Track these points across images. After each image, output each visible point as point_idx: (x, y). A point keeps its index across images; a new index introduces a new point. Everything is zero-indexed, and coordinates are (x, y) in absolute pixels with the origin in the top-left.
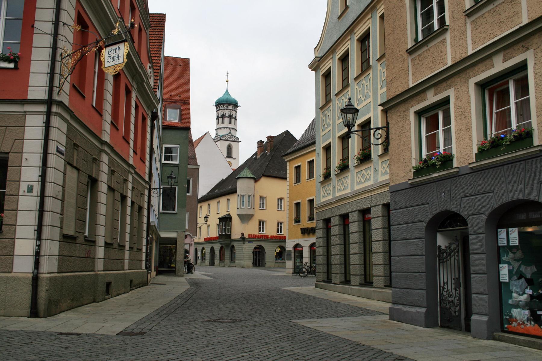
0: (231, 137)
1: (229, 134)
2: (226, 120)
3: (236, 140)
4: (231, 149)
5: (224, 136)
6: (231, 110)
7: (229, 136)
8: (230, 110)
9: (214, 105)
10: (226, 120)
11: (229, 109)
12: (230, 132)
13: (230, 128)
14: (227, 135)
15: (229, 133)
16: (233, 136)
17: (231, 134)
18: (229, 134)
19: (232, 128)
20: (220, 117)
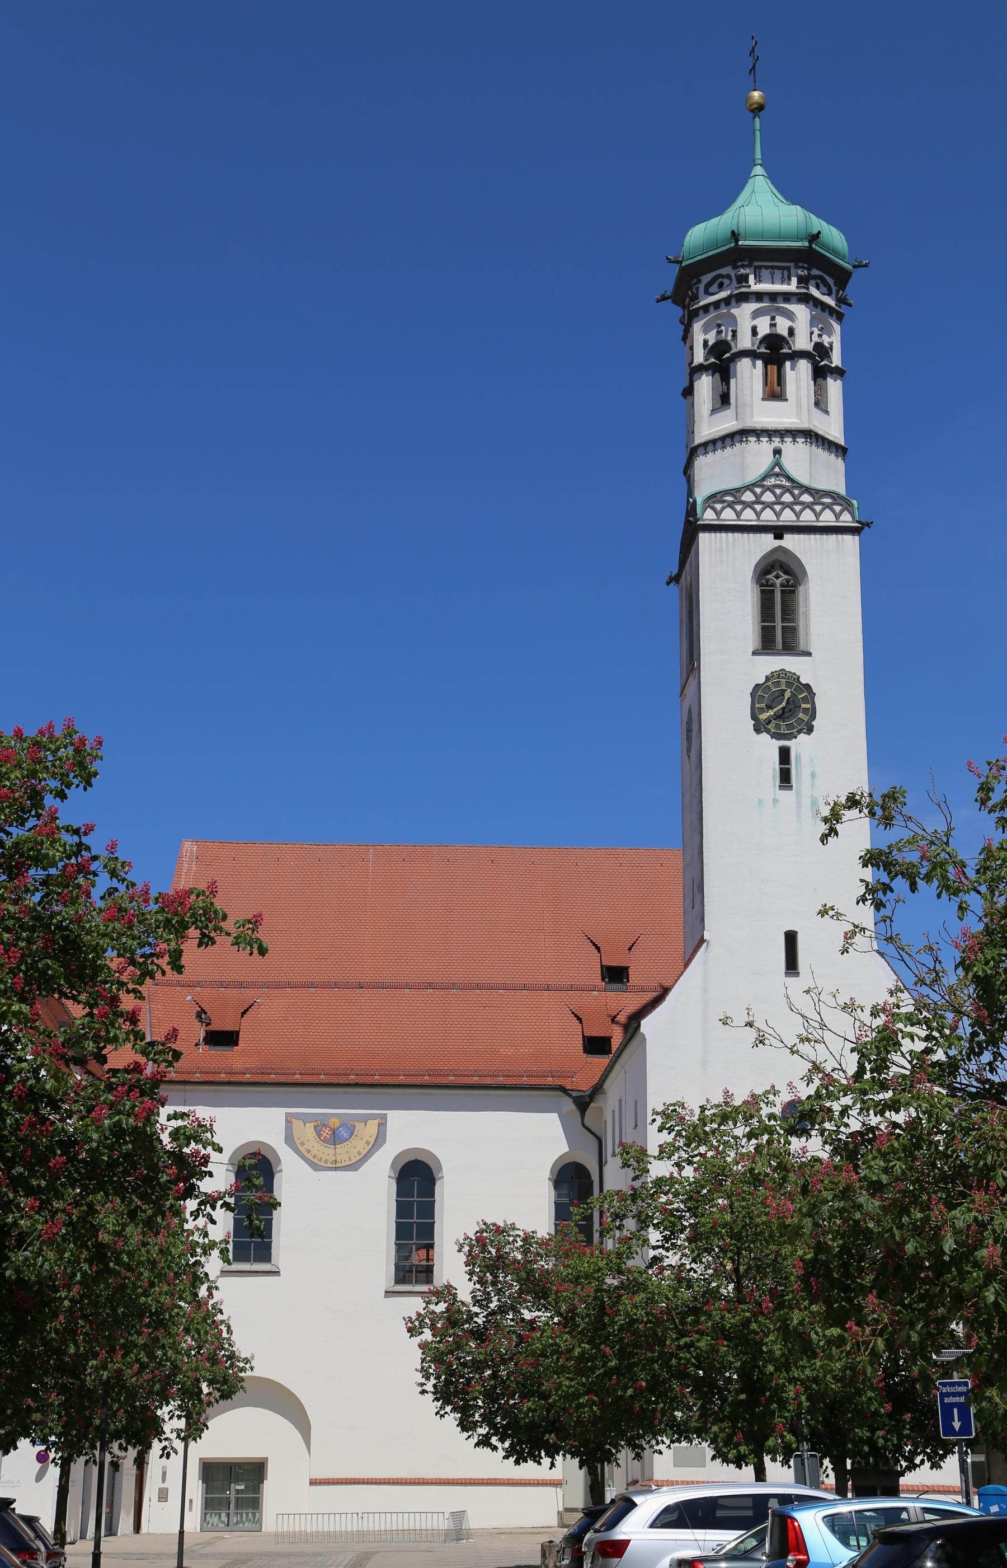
0: (787, 498)
1: (771, 481)
4: (790, 591)
5: (729, 498)
6: (773, 296)
9: (664, 298)
12: (778, 464)
14: (749, 487)
18: (771, 481)
19: (794, 434)
20: (701, 368)
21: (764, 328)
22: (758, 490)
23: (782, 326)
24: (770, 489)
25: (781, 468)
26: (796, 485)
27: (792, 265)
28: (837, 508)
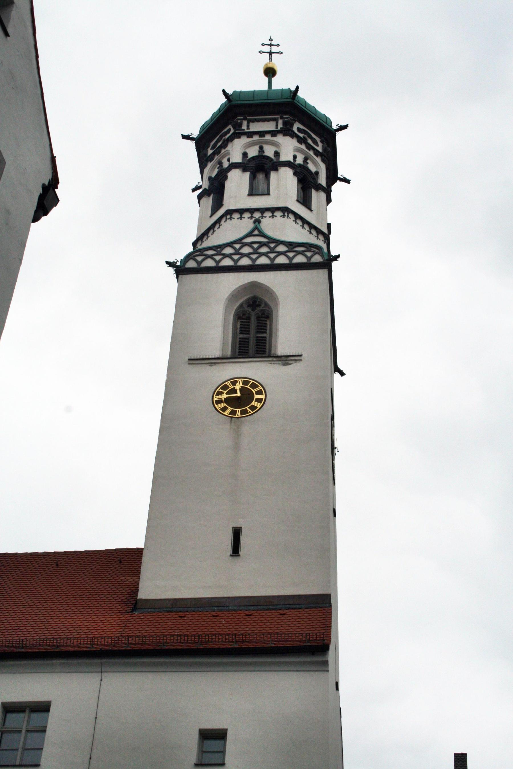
3: (300, 259)
6: (262, 134)
7: (246, 250)
8: (256, 138)
11: (250, 135)
13: (252, 211)
15: (250, 234)
16: (279, 242)
17: (262, 234)
19: (273, 210)
21: (253, 152)
22: (237, 246)
23: (269, 151)
24: (250, 244)
25: (259, 231)
26: (271, 241)
28: (309, 254)
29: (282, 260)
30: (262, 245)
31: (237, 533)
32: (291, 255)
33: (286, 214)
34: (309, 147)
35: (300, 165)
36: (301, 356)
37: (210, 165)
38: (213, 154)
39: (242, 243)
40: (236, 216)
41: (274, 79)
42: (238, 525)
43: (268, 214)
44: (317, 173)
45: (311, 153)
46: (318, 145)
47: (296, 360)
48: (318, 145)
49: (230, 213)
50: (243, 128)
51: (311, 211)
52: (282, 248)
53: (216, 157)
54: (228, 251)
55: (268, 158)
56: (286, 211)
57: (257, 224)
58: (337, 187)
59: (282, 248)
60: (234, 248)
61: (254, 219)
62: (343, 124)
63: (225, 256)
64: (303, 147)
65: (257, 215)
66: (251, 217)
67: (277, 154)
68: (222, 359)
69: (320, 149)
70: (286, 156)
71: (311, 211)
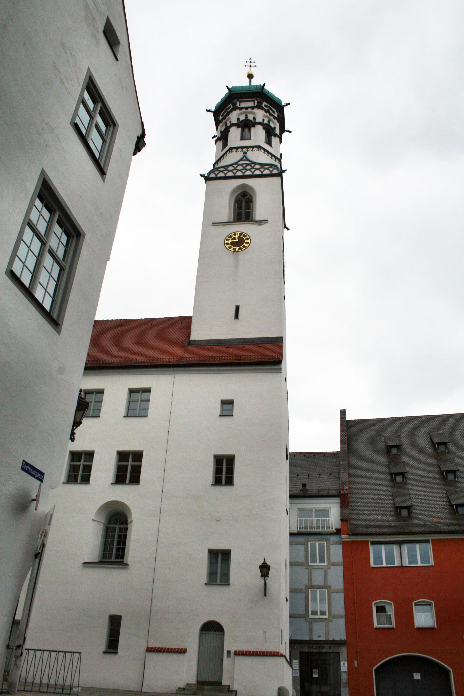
2: (235, 133)
3: (267, 172)
6: (247, 108)
7: (240, 168)
8: (244, 110)
10: (235, 133)
11: (241, 109)
13: (242, 148)
14: (231, 165)
15: (241, 160)
16: (256, 164)
17: (247, 160)
19: (253, 147)
21: (242, 118)
22: (235, 166)
23: (250, 117)
25: (246, 158)
27: (255, 99)
28: (271, 169)
29: (257, 172)
30: (247, 165)
31: (237, 308)
32: (262, 170)
33: (259, 149)
34: (271, 115)
35: (266, 124)
36: (267, 220)
37: (221, 125)
38: (222, 119)
39: (238, 164)
40: (234, 150)
41: (252, 80)
42: (237, 304)
43: (250, 149)
44: (275, 128)
45: (272, 118)
46: (275, 113)
47: (265, 223)
48: (275, 113)
49: (231, 149)
50: (237, 105)
51: (272, 147)
52: (257, 166)
53: (224, 121)
54: (231, 168)
55: (250, 121)
56: (259, 147)
57: (245, 154)
58: (285, 135)
59: (257, 166)
60: (234, 167)
61: (243, 152)
62: (288, 103)
63: (229, 171)
64: (268, 114)
65: (245, 150)
66: (242, 151)
67: (254, 118)
68: (229, 223)
69: (276, 115)
70: (259, 120)
71: (272, 147)
